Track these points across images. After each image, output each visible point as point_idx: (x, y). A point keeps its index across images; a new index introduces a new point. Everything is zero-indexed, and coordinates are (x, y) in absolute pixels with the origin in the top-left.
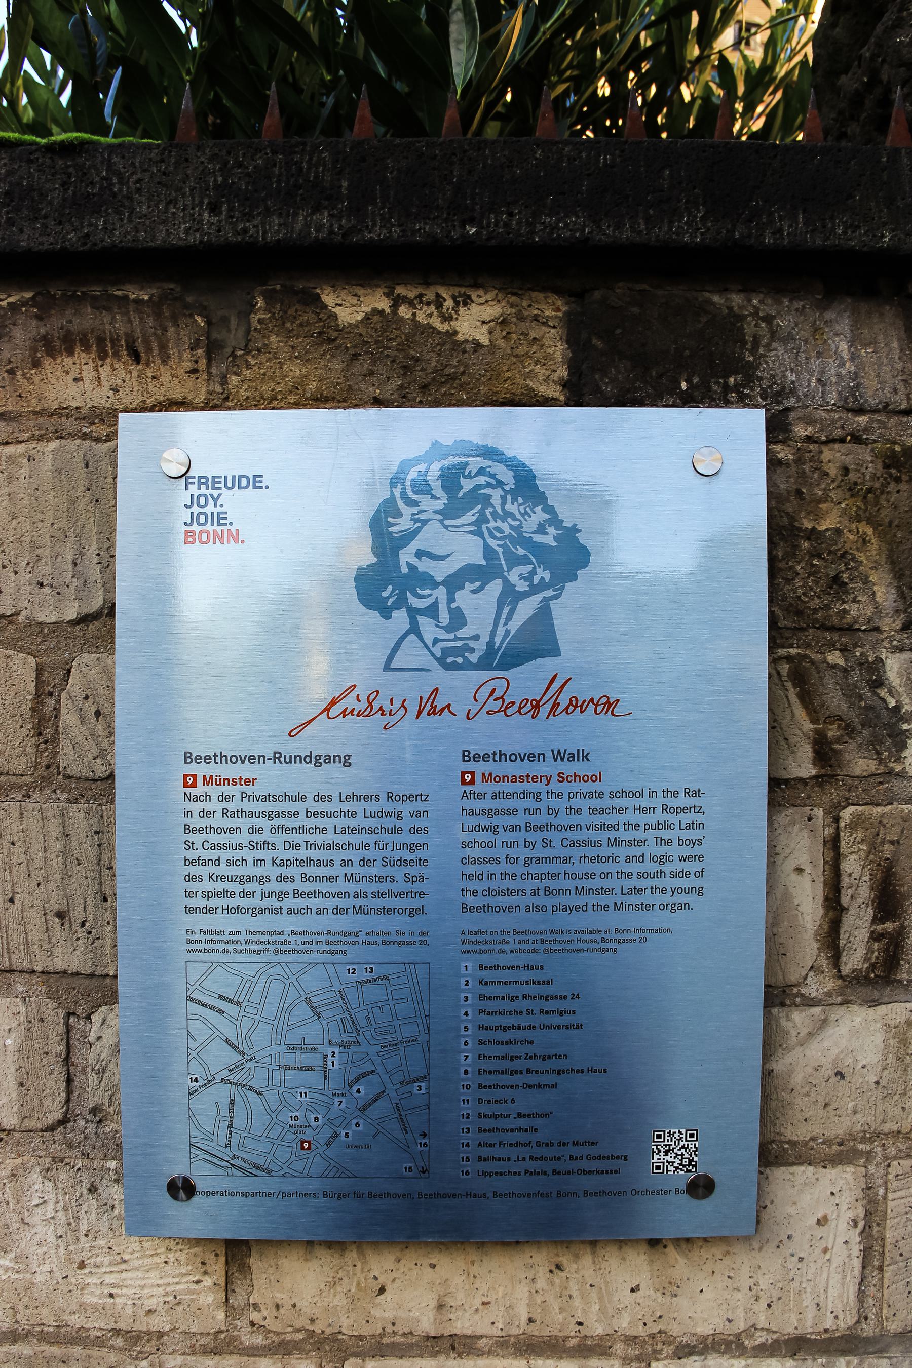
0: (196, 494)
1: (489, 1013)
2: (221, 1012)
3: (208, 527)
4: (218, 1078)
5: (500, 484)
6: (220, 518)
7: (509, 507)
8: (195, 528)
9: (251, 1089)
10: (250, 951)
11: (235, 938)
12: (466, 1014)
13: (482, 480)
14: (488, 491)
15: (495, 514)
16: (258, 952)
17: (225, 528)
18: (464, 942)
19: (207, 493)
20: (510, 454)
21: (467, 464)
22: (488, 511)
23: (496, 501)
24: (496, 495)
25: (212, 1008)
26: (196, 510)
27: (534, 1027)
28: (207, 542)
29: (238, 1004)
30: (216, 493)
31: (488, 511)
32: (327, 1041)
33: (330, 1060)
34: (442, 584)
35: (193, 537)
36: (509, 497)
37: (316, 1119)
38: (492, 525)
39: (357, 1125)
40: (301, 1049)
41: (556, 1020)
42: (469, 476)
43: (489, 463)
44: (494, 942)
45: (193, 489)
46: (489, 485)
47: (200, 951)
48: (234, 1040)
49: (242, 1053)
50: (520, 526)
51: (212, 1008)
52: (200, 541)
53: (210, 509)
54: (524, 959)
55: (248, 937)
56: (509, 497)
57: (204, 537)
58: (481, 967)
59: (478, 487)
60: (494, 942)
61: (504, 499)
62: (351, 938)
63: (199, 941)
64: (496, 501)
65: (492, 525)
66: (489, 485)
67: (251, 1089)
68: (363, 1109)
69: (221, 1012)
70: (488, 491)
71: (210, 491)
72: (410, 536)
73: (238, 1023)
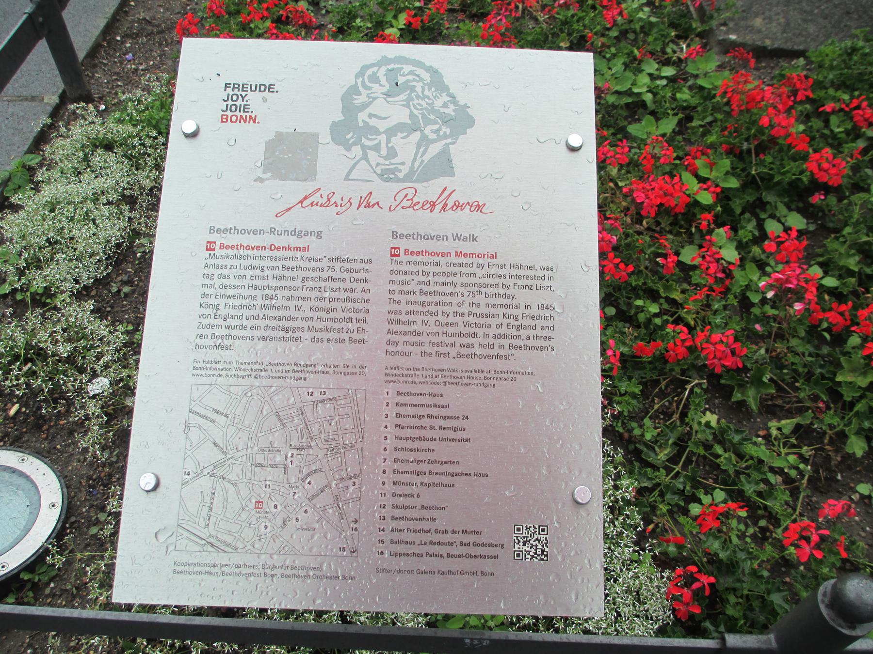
0: (231, 93)
1: (403, 427)
2: (213, 421)
3: (237, 113)
4: (205, 472)
5: (422, 80)
6: (245, 108)
7: (426, 92)
8: (229, 113)
9: (229, 481)
10: (237, 376)
11: (228, 366)
12: (386, 427)
13: (410, 77)
14: (414, 83)
15: (418, 97)
16: (243, 377)
17: (248, 114)
18: (386, 375)
19: (239, 93)
20: (428, 64)
21: (402, 68)
22: (414, 95)
23: (419, 89)
24: (419, 87)
25: (207, 418)
26: (230, 103)
27: (435, 439)
28: (236, 121)
29: (226, 416)
30: (244, 94)
31: (414, 95)
32: (288, 447)
33: (289, 459)
34: (383, 132)
35: (227, 119)
36: (427, 87)
37: (276, 507)
38: (416, 102)
39: (306, 512)
40: (269, 451)
41: (451, 435)
42: (403, 75)
43: (415, 68)
44: (408, 375)
45: (230, 91)
46: (414, 80)
47: (201, 375)
48: (220, 442)
49: (225, 453)
50: (433, 103)
51: (207, 418)
52: (231, 121)
53: (238, 103)
54: (426, 389)
55: (238, 366)
56: (427, 87)
57: (234, 119)
58: (398, 393)
59: (409, 81)
60: (408, 375)
61: (423, 89)
62: (309, 369)
63: (202, 368)
64: (419, 89)
65: (416, 102)
66: (414, 80)
67: (229, 481)
68: (311, 499)
69: (213, 421)
70: (414, 83)
71: (241, 92)
72: (365, 106)
73: (224, 430)
